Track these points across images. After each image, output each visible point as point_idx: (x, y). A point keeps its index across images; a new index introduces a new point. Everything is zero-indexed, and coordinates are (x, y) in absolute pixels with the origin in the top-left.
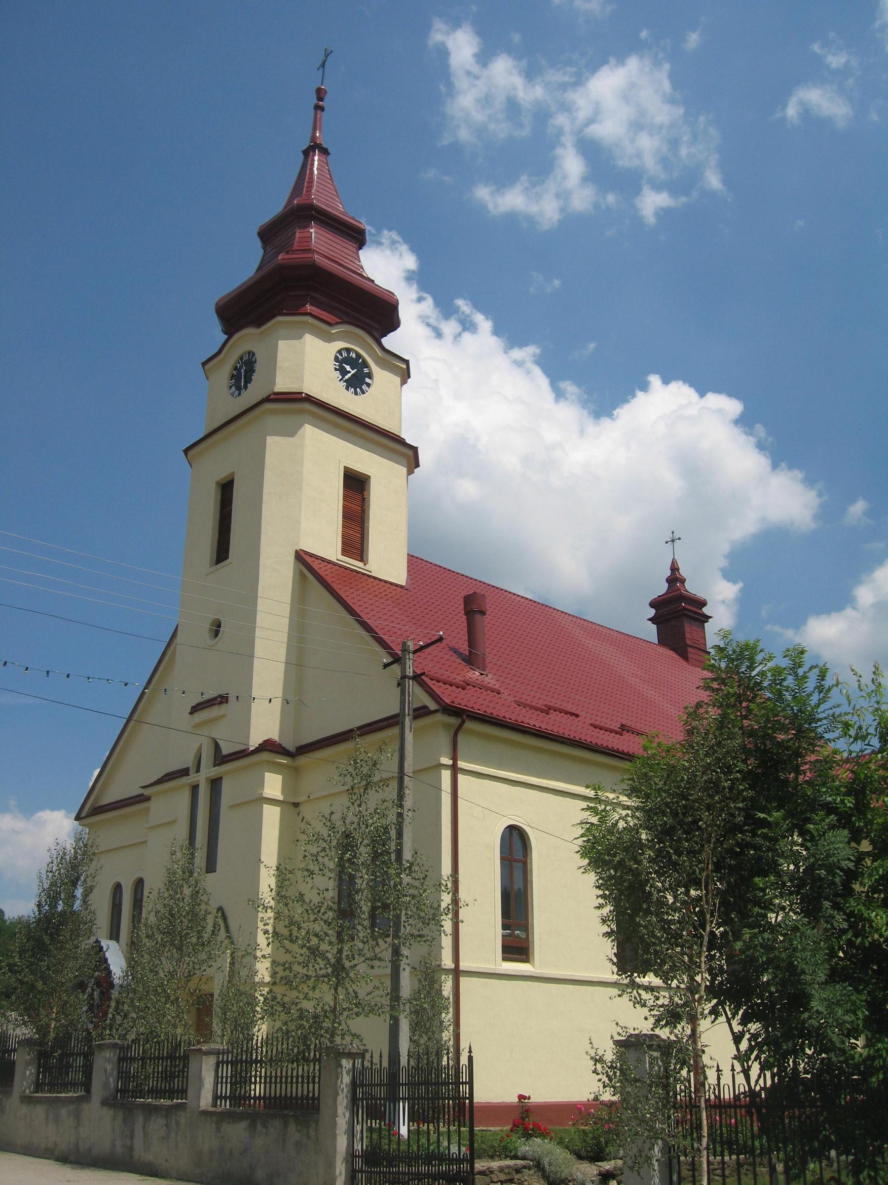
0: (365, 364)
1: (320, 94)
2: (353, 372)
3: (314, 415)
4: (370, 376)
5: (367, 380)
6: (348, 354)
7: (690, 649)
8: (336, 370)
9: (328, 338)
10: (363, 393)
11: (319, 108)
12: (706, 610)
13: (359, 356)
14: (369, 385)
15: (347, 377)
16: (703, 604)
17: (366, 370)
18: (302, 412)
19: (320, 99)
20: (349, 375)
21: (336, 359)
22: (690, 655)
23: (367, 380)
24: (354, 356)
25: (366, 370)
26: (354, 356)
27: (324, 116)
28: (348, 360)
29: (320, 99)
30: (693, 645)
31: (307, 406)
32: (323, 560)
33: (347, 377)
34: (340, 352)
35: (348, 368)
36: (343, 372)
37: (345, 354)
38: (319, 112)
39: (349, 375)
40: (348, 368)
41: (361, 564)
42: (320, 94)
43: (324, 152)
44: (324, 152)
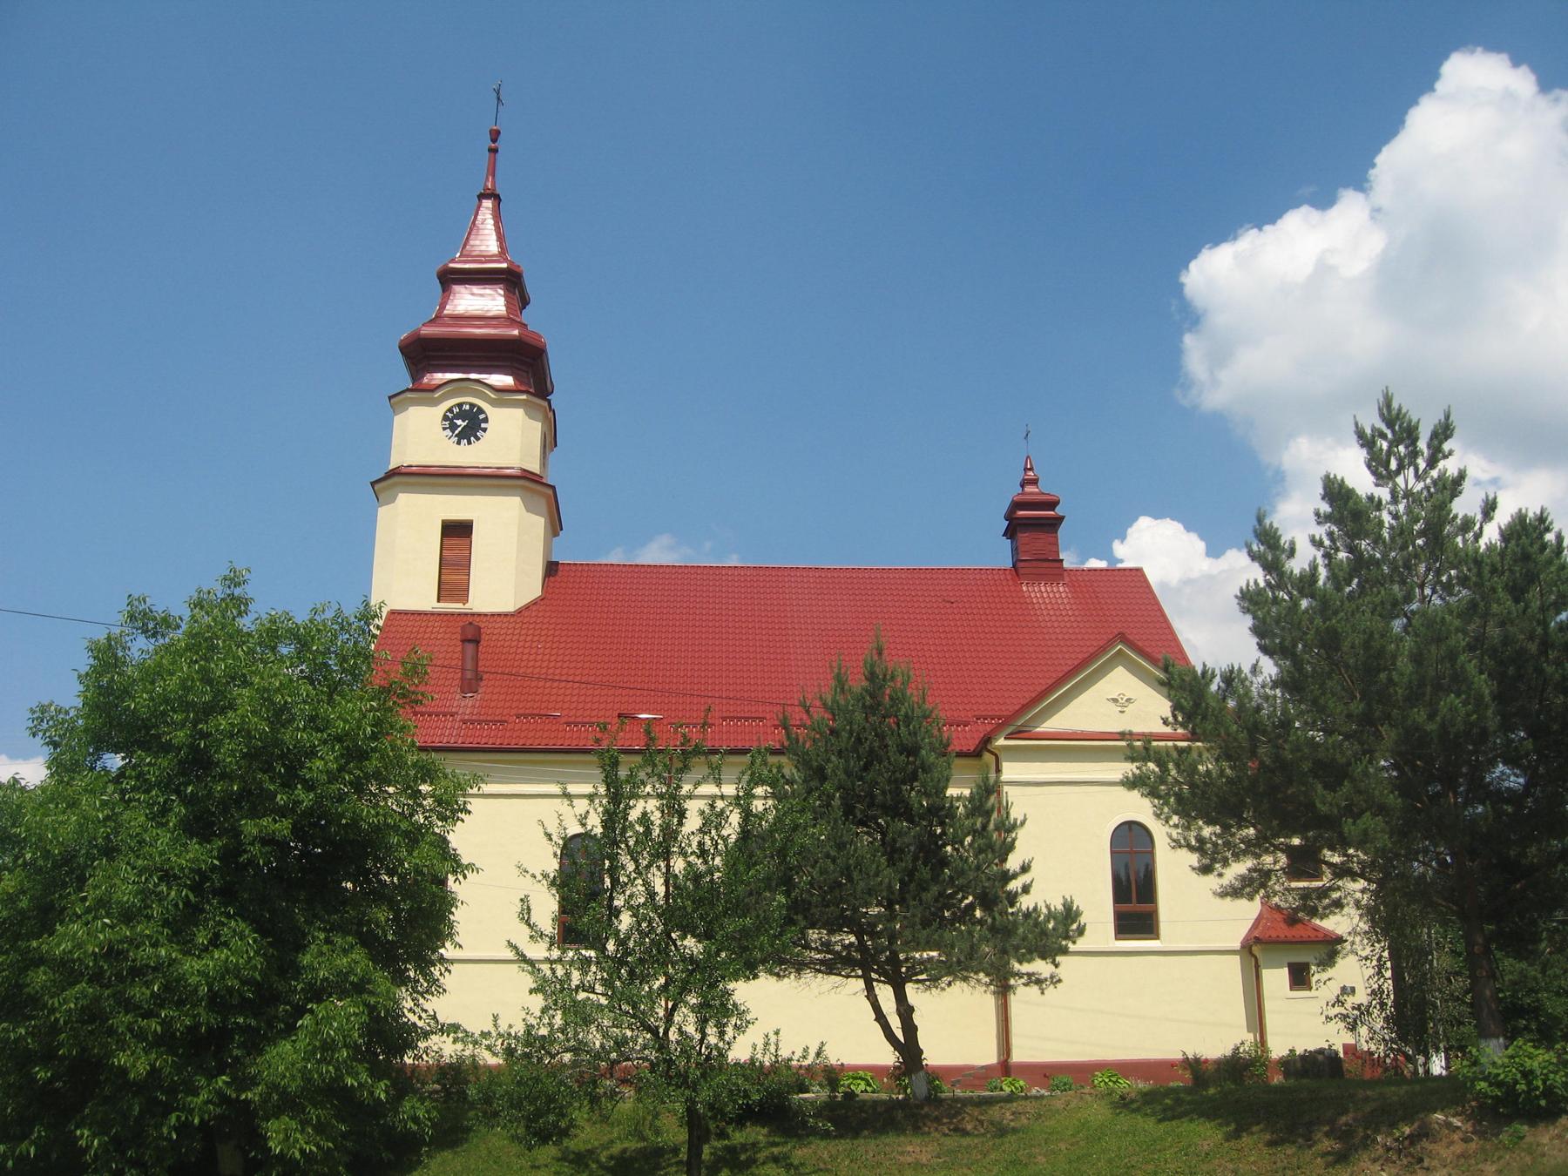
0: (481, 411)
1: (495, 136)
2: (465, 424)
3: (407, 484)
4: (486, 420)
5: (483, 425)
6: (460, 409)
7: (1021, 564)
8: (444, 429)
9: (435, 403)
10: (478, 439)
11: (494, 151)
12: (1059, 511)
13: (472, 405)
14: (485, 430)
15: (457, 432)
16: (1052, 505)
17: (482, 417)
18: (395, 485)
19: (494, 140)
20: (460, 429)
21: (445, 418)
22: (1021, 571)
23: (483, 425)
24: (468, 407)
25: (482, 417)
26: (468, 407)
27: (498, 155)
28: (462, 415)
29: (494, 140)
30: (1036, 557)
31: (396, 479)
32: (413, 613)
33: (457, 432)
34: (450, 410)
35: (459, 422)
36: (453, 427)
37: (456, 410)
38: (492, 154)
39: (460, 429)
40: (459, 422)
41: (460, 605)
42: (495, 136)
43: (496, 198)
44: (496, 198)
